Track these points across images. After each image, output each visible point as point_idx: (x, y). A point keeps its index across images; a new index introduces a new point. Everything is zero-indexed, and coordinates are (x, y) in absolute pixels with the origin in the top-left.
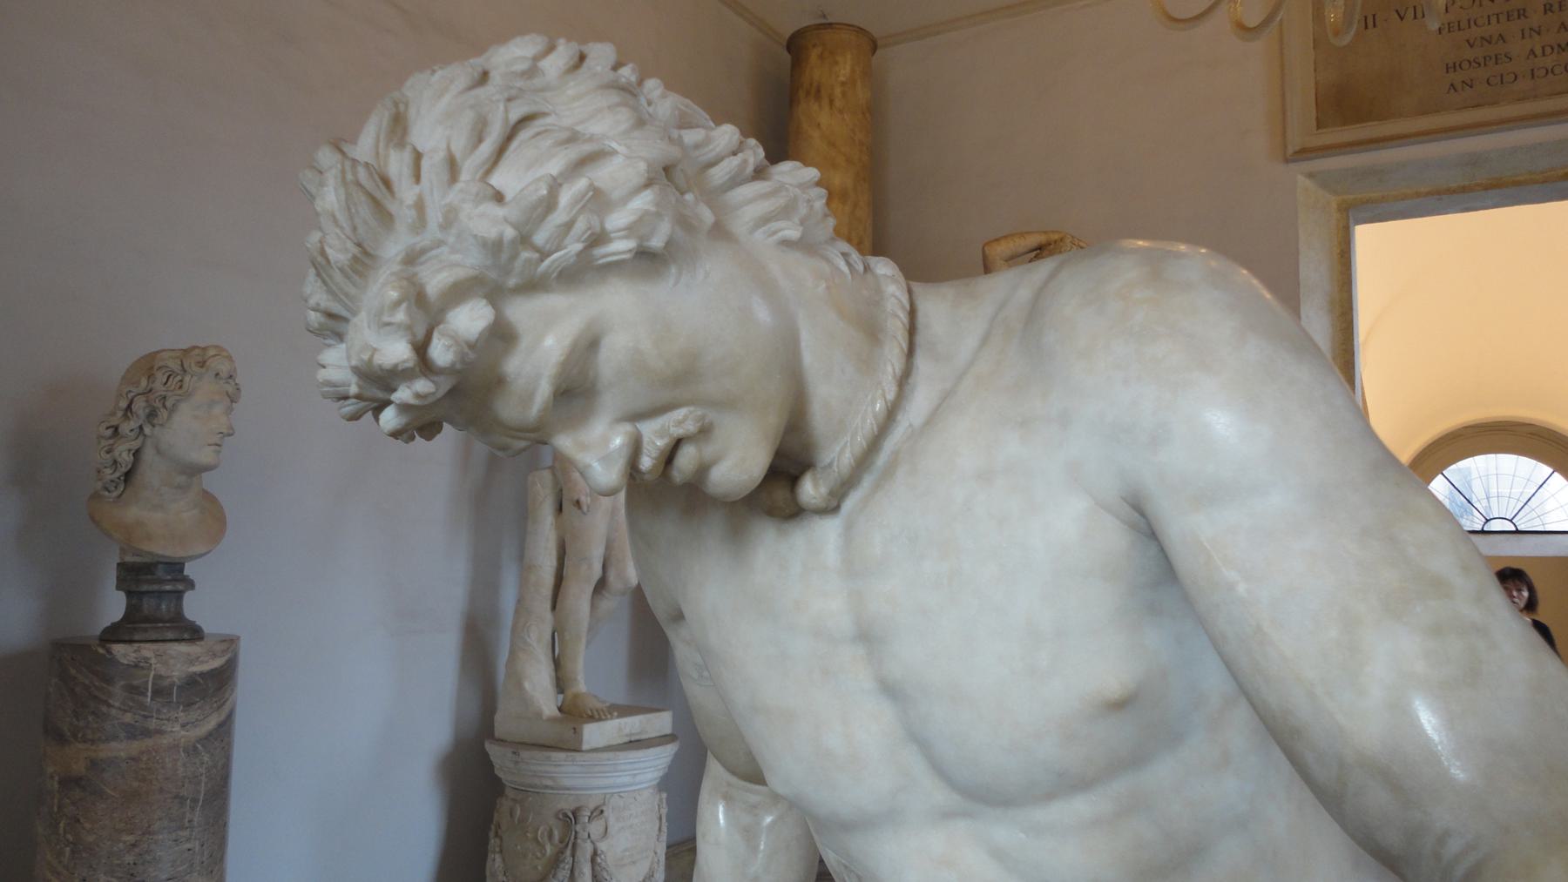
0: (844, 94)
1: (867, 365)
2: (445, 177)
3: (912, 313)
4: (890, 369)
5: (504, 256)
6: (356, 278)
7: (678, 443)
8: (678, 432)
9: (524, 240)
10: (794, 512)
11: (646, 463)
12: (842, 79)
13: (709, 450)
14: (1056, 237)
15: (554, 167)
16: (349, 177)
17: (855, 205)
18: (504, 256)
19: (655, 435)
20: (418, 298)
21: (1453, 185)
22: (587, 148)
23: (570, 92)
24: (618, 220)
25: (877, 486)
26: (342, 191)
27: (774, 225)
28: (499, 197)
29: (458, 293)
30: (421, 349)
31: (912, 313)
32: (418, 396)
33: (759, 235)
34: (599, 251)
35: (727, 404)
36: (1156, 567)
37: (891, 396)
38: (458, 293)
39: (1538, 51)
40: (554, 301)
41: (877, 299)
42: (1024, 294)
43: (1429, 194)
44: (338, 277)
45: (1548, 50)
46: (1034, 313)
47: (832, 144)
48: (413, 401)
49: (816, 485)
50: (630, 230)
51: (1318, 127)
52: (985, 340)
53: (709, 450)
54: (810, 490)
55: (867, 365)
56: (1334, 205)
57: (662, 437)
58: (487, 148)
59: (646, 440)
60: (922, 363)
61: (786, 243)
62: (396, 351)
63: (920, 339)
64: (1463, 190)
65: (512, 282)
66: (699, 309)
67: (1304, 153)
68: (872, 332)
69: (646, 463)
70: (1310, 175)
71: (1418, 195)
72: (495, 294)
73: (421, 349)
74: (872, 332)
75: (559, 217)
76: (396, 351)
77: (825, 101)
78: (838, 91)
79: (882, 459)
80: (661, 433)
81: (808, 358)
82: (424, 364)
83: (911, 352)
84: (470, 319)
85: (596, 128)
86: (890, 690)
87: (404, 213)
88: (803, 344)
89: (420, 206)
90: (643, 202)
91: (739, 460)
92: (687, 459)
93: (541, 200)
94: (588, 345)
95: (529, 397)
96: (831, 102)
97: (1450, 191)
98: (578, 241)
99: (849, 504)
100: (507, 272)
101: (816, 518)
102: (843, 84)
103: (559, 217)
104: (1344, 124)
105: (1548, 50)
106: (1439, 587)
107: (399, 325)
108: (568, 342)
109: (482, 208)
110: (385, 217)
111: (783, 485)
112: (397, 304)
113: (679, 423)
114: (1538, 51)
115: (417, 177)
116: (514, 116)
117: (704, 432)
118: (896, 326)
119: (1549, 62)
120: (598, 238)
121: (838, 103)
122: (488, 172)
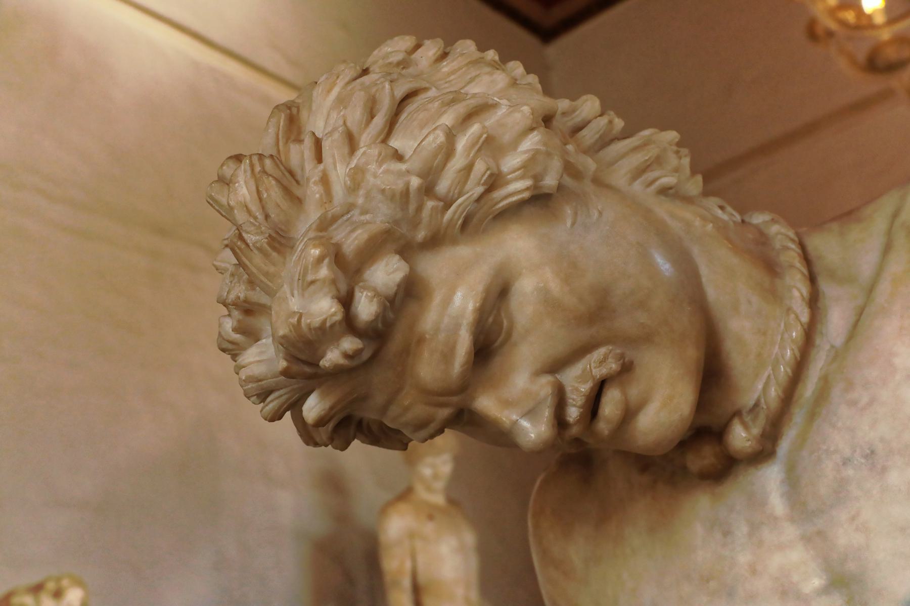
1: (773, 295)
2: (346, 150)
3: (802, 246)
4: (796, 294)
5: (412, 207)
6: (274, 254)
7: (600, 387)
8: (599, 372)
9: (428, 190)
10: (727, 467)
11: (573, 413)
13: (634, 392)
15: (448, 119)
16: (258, 168)
18: (412, 207)
19: (577, 382)
20: (338, 258)
22: (472, 102)
23: (445, 69)
24: (511, 162)
25: (812, 416)
26: (252, 184)
27: (650, 175)
28: (398, 157)
29: (372, 251)
30: (346, 301)
31: (802, 246)
32: (346, 356)
33: (637, 186)
34: (497, 194)
35: (646, 338)
37: (805, 318)
38: (372, 251)
40: (463, 251)
41: (763, 239)
44: (258, 258)
48: (342, 361)
49: (746, 427)
50: (525, 166)
53: (634, 392)
54: (741, 437)
55: (773, 295)
57: (585, 382)
58: (379, 121)
59: (568, 389)
60: (827, 287)
61: (664, 191)
62: (324, 307)
63: (818, 267)
65: (421, 235)
66: (602, 243)
68: (771, 267)
69: (573, 413)
72: (407, 251)
73: (346, 301)
74: (771, 267)
75: (457, 162)
76: (324, 307)
79: (809, 388)
80: (582, 379)
81: (712, 293)
82: (349, 324)
83: (812, 279)
84: (386, 273)
85: (475, 89)
87: (314, 192)
88: (704, 280)
89: (325, 181)
90: (532, 142)
91: (662, 405)
92: (610, 406)
93: (440, 147)
94: (499, 293)
95: (448, 356)
98: (478, 184)
99: (784, 446)
100: (415, 224)
101: (752, 470)
103: (457, 162)
107: (324, 281)
108: (480, 288)
109: (384, 167)
111: (706, 452)
112: (320, 260)
113: (602, 362)
115: (319, 159)
116: (400, 93)
117: (627, 369)
118: (792, 256)
120: (494, 182)
122: (385, 141)
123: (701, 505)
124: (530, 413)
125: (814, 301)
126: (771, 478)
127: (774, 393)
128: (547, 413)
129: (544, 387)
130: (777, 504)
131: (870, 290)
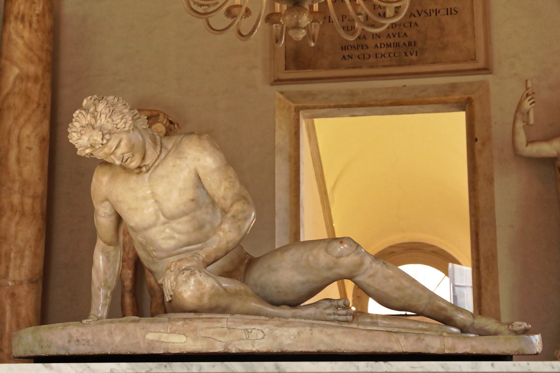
0: (38, 21)
1: (155, 149)
12: (37, 12)
14: (156, 113)
17: (43, 85)
21: (345, 104)
24: (128, 125)
30: (102, 139)
36: (199, 182)
38: (106, 134)
39: (379, 46)
40: (117, 135)
41: (155, 138)
42: (179, 139)
43: (335, 107)
45: (383, 46)
46: (180, 142)
47: (31, 49)
51: (286, 69)
52: (173, 146)
54: (144, 169)
56: (293, 109)
58: (110, 113)
60: (163, 150)
61: (144, 128)
64: (349, 106)
67: (278, 81)
70: (282, 93)
71: (329, 107)
77: (27, 24)
78: (35, 19)
86: (156, 201)
87: (99, 122)
92: (129, 161)
96: (31, 25)
97: (343, 107)
99: (150, 172)
102: (38, 15)
104: (297, 69)
105: (383, 46)
106: (231, 177)
110: (96, 122)
114: (379, 46)
117: (133, 156)
118: (159, 143)
119: (383, 51)
121: (35, 25)
123: (134, 177)
124: (118, 160)
125: (160, 152)
126: (147, 175)
127: (151, 164)
128: (121, 160)
129: (121, 156)
130: (147, 180)
131: (169, 151)
